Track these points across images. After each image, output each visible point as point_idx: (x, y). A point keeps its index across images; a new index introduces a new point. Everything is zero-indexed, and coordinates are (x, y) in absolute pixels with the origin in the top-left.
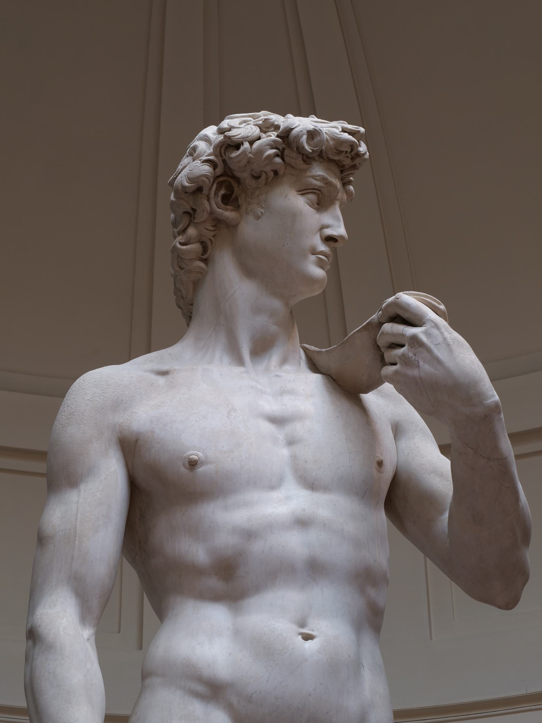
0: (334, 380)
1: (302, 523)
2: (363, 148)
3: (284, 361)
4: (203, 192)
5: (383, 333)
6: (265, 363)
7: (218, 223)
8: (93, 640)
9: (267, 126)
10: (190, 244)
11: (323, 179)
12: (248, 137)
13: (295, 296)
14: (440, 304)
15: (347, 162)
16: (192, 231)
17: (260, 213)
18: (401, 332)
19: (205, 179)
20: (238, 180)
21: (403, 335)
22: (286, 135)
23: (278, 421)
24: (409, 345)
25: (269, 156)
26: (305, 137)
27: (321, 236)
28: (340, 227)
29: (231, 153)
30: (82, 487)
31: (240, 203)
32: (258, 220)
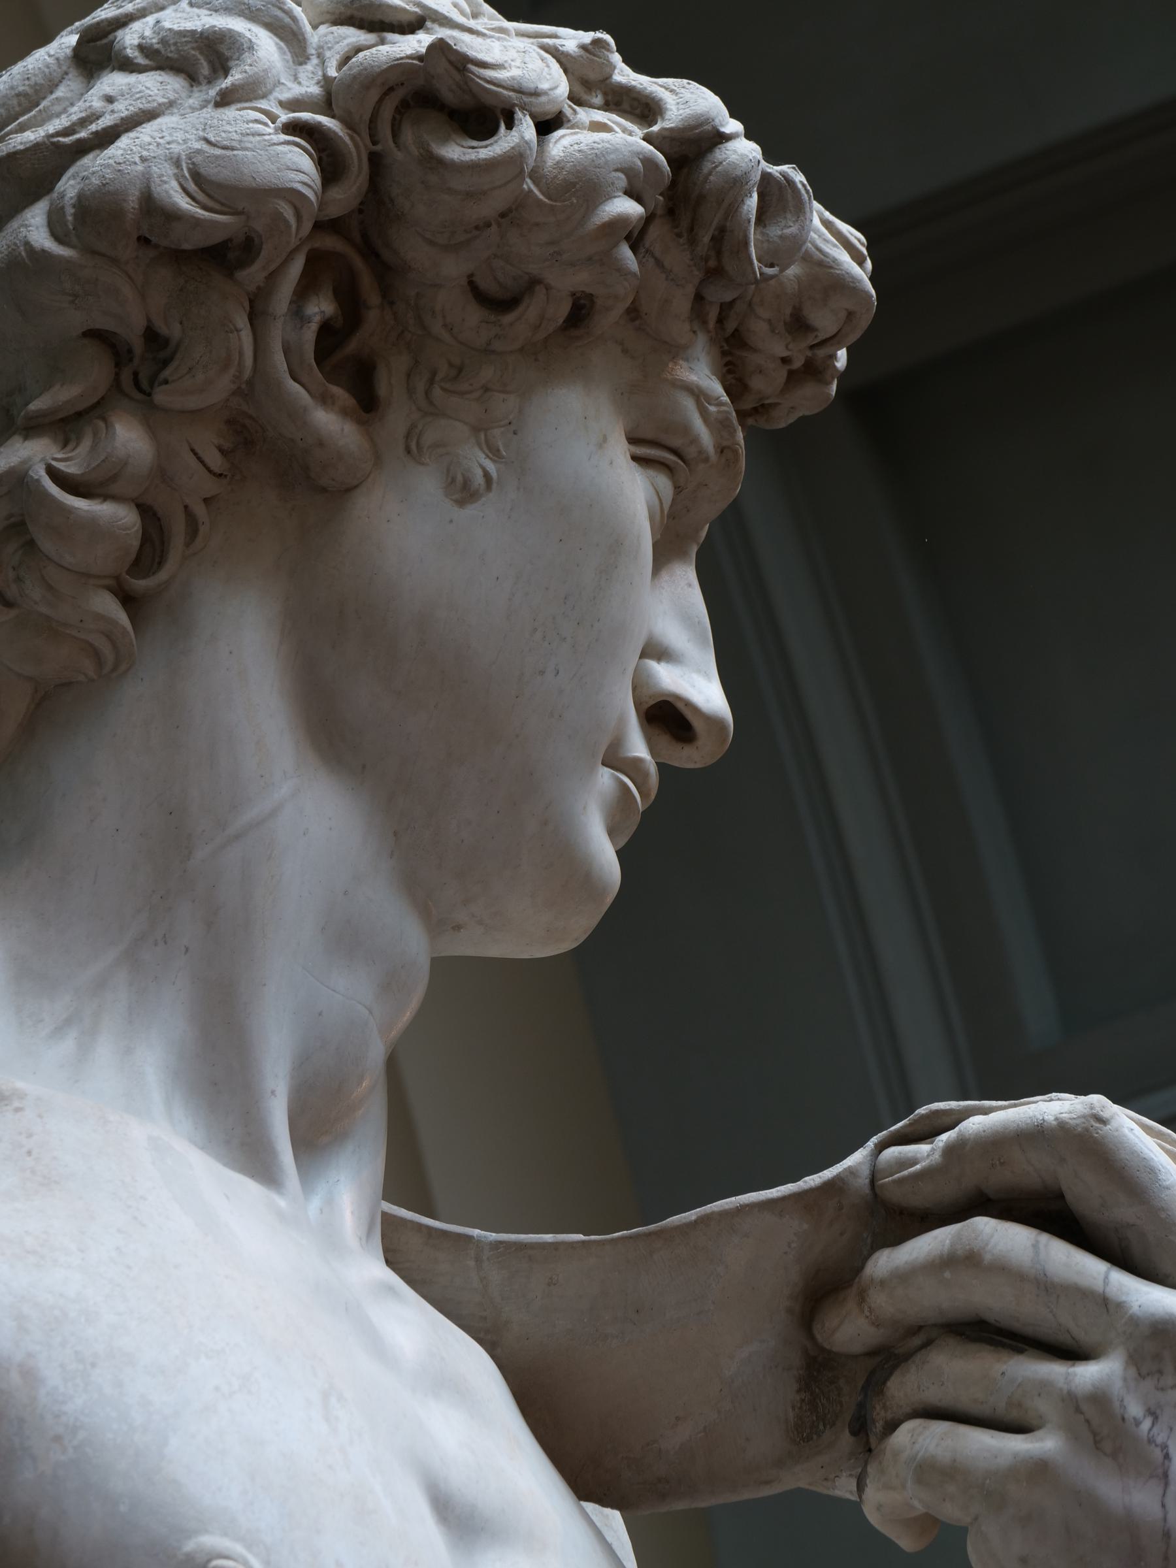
4: (241, 275)
5: (967, 1261)
6: (315, 1204)
7: (254, 444)
9: (593, 76)
10: (106, 497)
12: (536, 93)
13: (458, 928)
16: (128, 438)
17: (479, 479)
18: (1098, 1286)
19: (288, 213)
21: (1106, 1305)
24: (1134, 1359)
25: (617, 224)
27: (634, 689)
29: (445, 140)
31: (382, 390)
32: (461, 503)
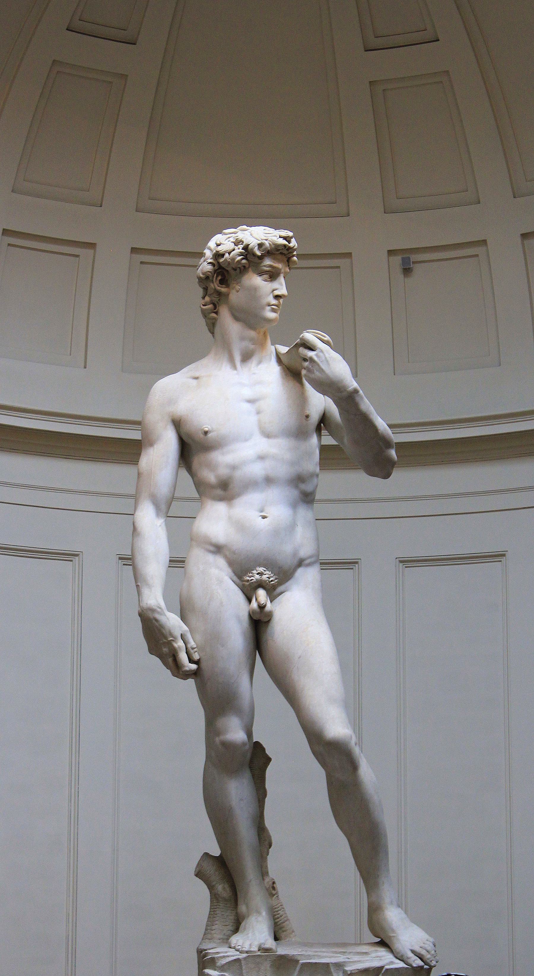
0: (288, 368)
1: (261, 458)
2: (293, 243)
3: (260, 362)
7: (219, 294)
8: (164, 524)
11: (270, 266)
14: (325, 337)
15: (285, 252)
16: (207, 299)
20: (227, 271)
22: (246, 248)
23: (251, 401)
26: (257, 248)
28: (282, 289)
30: (155, 446)
